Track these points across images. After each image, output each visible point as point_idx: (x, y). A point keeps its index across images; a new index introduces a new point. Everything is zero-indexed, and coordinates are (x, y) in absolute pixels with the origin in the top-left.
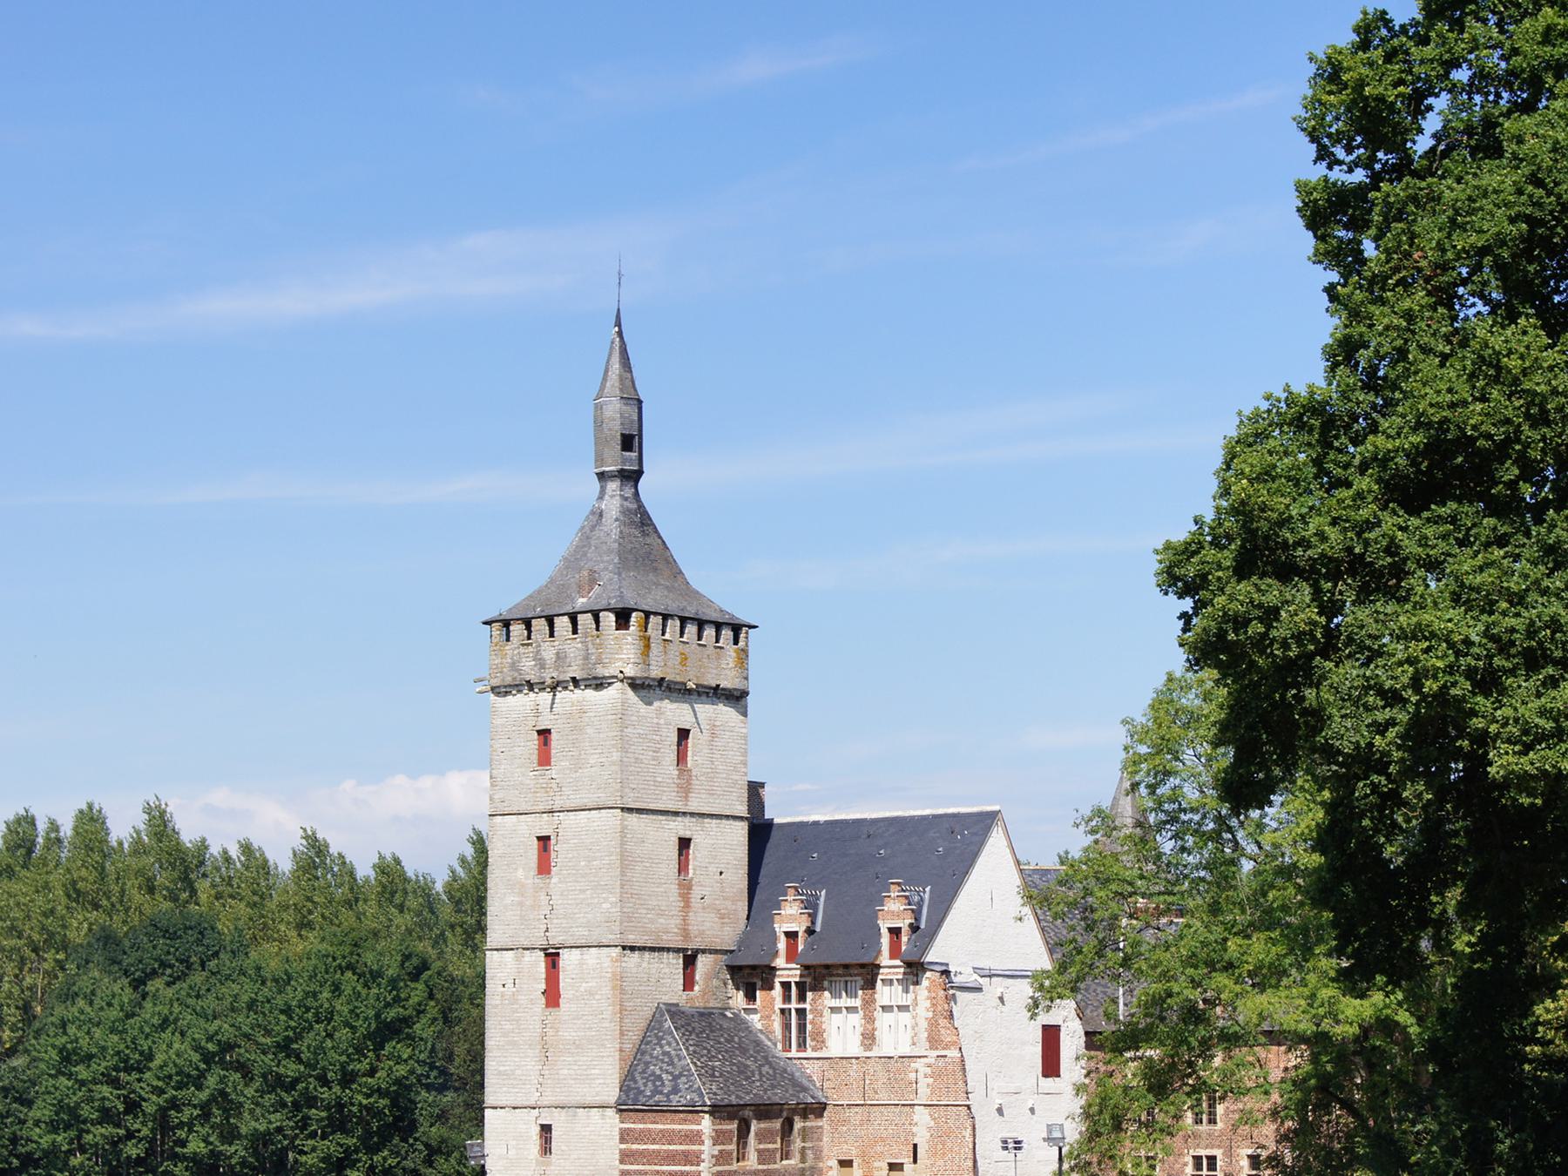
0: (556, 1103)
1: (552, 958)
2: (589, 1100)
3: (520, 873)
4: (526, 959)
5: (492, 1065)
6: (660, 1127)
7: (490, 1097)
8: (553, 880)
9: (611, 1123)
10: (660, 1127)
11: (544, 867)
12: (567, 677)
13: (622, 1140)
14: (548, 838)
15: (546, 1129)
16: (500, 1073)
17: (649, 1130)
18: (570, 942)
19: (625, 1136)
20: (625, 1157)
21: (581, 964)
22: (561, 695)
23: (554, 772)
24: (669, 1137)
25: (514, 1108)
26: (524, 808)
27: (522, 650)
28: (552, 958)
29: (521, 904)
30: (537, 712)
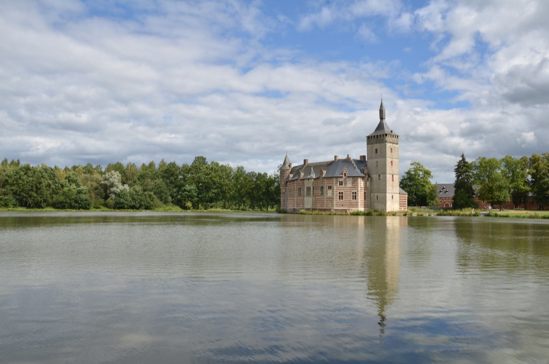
1: (393, 176)
7: (387, 192)
9: (399, 194)
11: (392, 165)
15: (392, 196)
19: (400, 197)
20: (400, 199)
21: (396, 177)
22: (393, 144)
24: (404, 197)
28: (393, 176)
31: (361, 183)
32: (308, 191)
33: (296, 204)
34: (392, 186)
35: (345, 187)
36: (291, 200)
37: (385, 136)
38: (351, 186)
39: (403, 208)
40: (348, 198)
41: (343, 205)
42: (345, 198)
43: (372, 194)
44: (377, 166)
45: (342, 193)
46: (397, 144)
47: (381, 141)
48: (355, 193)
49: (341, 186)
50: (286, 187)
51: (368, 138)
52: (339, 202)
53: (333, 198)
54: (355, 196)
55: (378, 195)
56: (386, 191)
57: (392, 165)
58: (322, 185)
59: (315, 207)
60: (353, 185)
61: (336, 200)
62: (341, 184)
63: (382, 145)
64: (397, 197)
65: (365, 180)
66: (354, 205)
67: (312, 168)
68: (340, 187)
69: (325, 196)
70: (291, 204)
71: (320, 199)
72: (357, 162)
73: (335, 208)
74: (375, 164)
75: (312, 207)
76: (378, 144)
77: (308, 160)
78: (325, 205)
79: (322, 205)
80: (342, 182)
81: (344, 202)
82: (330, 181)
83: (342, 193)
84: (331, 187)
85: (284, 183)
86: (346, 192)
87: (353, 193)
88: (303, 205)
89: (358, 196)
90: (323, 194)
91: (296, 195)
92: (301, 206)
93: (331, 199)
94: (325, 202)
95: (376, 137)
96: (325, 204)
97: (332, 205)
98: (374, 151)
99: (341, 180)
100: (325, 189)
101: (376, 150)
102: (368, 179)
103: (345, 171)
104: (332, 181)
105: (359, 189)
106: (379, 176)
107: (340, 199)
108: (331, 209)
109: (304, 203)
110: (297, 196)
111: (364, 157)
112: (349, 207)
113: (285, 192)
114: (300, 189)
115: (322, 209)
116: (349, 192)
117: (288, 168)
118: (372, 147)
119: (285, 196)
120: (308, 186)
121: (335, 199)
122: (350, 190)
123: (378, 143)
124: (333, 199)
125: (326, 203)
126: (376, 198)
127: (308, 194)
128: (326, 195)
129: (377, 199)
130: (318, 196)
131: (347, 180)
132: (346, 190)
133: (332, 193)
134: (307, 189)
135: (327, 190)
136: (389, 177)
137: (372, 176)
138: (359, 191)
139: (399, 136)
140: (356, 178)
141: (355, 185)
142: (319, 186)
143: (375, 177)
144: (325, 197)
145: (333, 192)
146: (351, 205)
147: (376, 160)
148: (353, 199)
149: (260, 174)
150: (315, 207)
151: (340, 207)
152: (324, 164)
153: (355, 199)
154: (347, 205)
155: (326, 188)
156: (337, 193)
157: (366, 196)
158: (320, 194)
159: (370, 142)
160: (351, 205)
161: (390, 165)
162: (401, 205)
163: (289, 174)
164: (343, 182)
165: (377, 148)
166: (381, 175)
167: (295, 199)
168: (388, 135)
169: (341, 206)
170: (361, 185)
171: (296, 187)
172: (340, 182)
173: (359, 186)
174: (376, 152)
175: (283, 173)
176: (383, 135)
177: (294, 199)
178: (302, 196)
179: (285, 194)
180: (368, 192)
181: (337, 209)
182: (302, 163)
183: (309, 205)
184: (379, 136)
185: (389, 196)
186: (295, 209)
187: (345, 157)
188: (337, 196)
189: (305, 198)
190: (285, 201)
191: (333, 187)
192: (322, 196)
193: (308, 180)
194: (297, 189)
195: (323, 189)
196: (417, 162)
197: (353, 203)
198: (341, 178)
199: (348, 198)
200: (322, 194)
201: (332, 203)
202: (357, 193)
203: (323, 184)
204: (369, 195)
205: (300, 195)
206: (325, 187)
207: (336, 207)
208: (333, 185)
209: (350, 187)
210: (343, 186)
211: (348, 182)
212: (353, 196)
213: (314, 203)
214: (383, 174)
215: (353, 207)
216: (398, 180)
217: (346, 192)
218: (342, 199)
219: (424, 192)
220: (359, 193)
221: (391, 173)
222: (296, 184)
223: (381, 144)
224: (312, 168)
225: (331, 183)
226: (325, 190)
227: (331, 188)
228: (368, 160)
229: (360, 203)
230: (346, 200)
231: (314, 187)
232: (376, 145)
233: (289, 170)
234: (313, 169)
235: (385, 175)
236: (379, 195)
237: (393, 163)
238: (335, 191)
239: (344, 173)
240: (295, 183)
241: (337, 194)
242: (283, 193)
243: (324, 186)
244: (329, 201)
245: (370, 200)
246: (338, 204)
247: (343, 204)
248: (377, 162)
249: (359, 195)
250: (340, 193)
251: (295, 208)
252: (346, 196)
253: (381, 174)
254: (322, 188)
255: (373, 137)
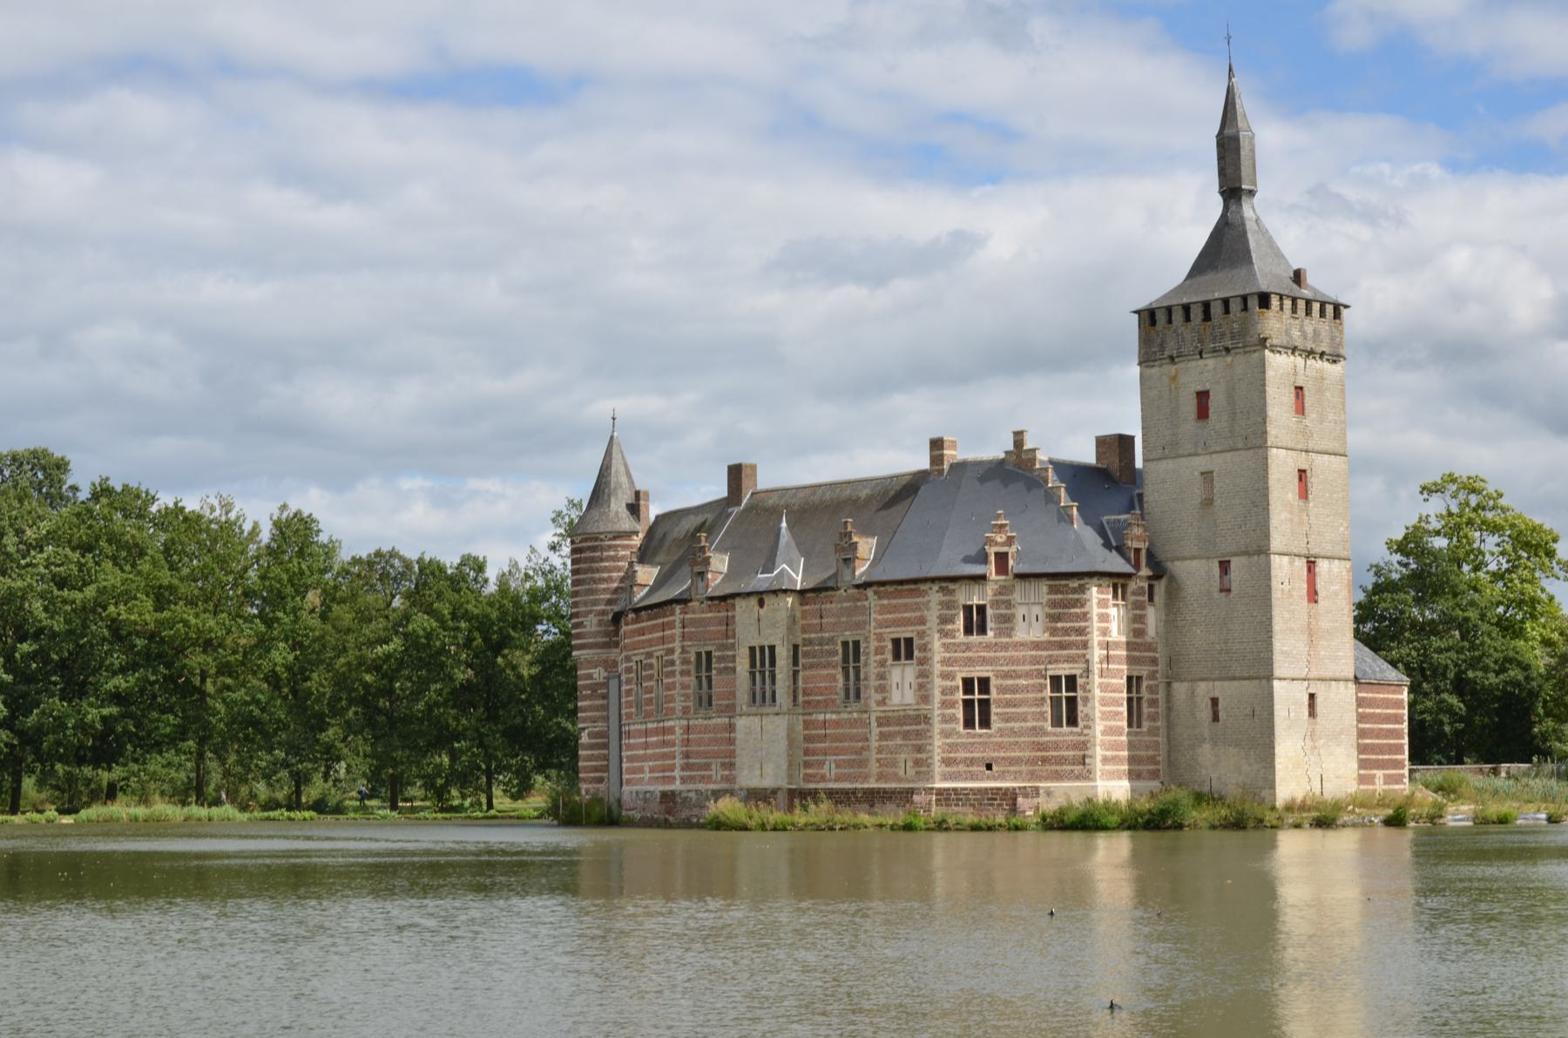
0: (1320, 677)
1: (1311, 565)
2: (1337, 675)
3: (1290, 495)
4: (1297, 564)
5: (1278, 645)
6: (1382, 696)
7: (1277, 672)
8: (1311, 505)
10: (1382, 696)
11: (1304, 494)
12: (1319, 350)
13: (1359, 706)
14: (1304, 471)
15: (1312, 696)
16: (1282, 652)
17: (1375, 698)
18: (1322, 554)
19: (1360, 703)
20: (1361, 718)
21: (1330, 571)
22: (1310, 362)
23: (1307, 422)
25: (1293, 680)
26: (1289, 446)
27: (1292, 321)
28: (1311, 565)
29: (1291, 520)
30: (1295, 373)
31: (1104, 618)
32: (762, 673)
33: (678, 762)
34: (1312, 634)
35: (1005, 647)
36: (647, 733)
37: (1253, 303)
38: (1046, 637)
39: (1379, 773)
40: (1023, 718)
41: (989, 767)
42: (1007, 718)
43: (1180, 689)
44: (1208, 502)
45: (984, 684)
46: (1335, 358)
47: (1229, 344)
48: (1072, 681)
49: (975, 638)
50: (614, 654)
51: (1149, 317)
52: (965, 746)
53: (927, 719)
54: (1072, 702)
55: (1217, 694)
56: (1268, 663)
57: (1304, 494)
58: (849, 636)
59: (808, 778)
60: (1054, 632)
61: (945, 734)
62: (976, 621)
63: (1239, 363)
64: (1340, 701)
65: (1132, 598)
66: (1060, 761)
67: (784, 524)
68: (968, 647)
69: (873, 706)
70: (647, 765)
71: (838, 724)
72: (1074, 474)
73: (938, 785)
74: (1197, 492)
75: (790, 776)
76: (1210, 363)
77: (753, 468)
78: (874, 768)
79: (850, 764)
80: (981, 609)
81: (1000, 746)
82: (907, 608)
83: (984, 684)
84: (909, 641)
85: (600, 623)
86: (1007, 675)
87: (1055, 680)
88: (731, 766)
89: (1086, 700)
90: (858, 696)
91: (678, 705)
92: (716, 772)
93: (913, 725)
94: (874, 744)
95: (1197, 314)
96: (874, 756)
97: (917, 763)
98: (1189, 407)
99: (976, 601)
100: (873, 659)
101: (1203, 396)
102: (1151, 587)
103: (1000, 538)
104: (917, 607)
105: (1097, 654)
106: (1225, 566)
107: (969, 723)
108: (911, 791)
109: (732, 754)
110: (686, 710)
111: (1125, 442)
112: (1033, 776)
113: (605, 685)
114: (705, 662)
115: (854, 791)
116: (1028, 675)
117: (626, 523)
118: (1174, 379)
119: (605, 708)
120: (756, 643)
121: (937, 727)
122: (1036, 661)
123: (1214, 351)
124: (923, 726)
125: (880, 751)
126: (1205, 714)
127: (762, 697)
128: (879, 697)
129: (1216, 718)
130: (826, 705)
131: (1016, 597)
132: (1012, 661)
133: (921, 686)
134: (753, 664)
135: (882, 664)
136: (1285, 572)
137: (1180, 568)
138: (1096, 668)
139: (1346, 307)
140: (1074, 584)
141: (1066, 632)
142: (831, 640)
143: (1195, 573)
144: (876, 711)
145: (923, 675)
146: (1044, 760)
147: (1201, 463)
148: (1057, 722)
149: (430, 570)
150: (808, 778)
151: (973, 777)
152: (864, 493)
153: (1073, 721)
154: (1013, 761)
155: (880, 650)
156: (948, 683)
157: (1139, 699)
158: (842, 694)
159: (1162, 347)
160: (1044, 760)
161: (1292, 495)
162: (1369, 757)
163: (631, 564)
164: (989, 612)
165: (1207, 386)
166: (1236, 563)
167: (671, 730)
168: (1275, 301)
169: (974, 769)
170: (1105, 632)
171: (677, 645)
172: (968, 609)
173: (1096, 638)
174: (1203, 413)
175: (593, 560)
176: (1245, 298)
177: (664, 731)
178: (721, 711)
179: (605, 697)
180: (1152, 676)
181: (955, 790)
182: (718, 489)
183: (769, 769)
184: (1217, 310)
185: (1287, 697)
186: (673, 792)
187: (995, 449)
188: (952, 705)
189: (741, 723)
190: (606, 746)
191: (924, 648)
192: (854, 706)
193: (761, 604)
194: (685, 662)
195: (857, 658)
196: (1462, 472)
197: (1056, 746)
198: (976, 588)
199: (1023, 718)
200: (854, 693)
201: (919, 749)
202: (1080, 681)
203: (859, 626)
204: (1161, 696)
205: (705, 701)
206: (873, 644)
207: (945, 778)
208: (922, 634)
209: (1037, 645)
210: (990, 634)
211: (1020, 611)
212: (1055, 703)
213: (805, 750)
214: (1246, 553)
215: (1058, 776)
216: (1345, 593)
217: (1007, 675)
218: (986, 723)
219: (1515, 673)
220: (1097, 680)
221: (1305, 552)
222: (677, 631)
223: (1229, 359)
224: (784, 524)
225: (909, 622)
226: (870, 667)
227: (910, 656)
228: (1152, 465)
229: (1103, 745)
230: (1012, 732)
231: (796, 647)
232: (1201, 362)
233: (629, 534)
234: (790, 527)
235: (1263, 557)
236: (1222, 690)
237: (1314, 482)
238: (938, 668)
239: (992, 551)
240: (671, 625)
241: (953, 690)
242: (594, 688)
243: (867, 639)
244: (899, 741)
245: (1170, 726)
246: (961, 755)
247: (990, 754)
248: (1207, 476)
249: (1097, 692)
250: (968, 685)
251: (677, 786)
252: (1009, 704)
253: (1236, 554)
254: (853, 652)
255: (1178, 316)
